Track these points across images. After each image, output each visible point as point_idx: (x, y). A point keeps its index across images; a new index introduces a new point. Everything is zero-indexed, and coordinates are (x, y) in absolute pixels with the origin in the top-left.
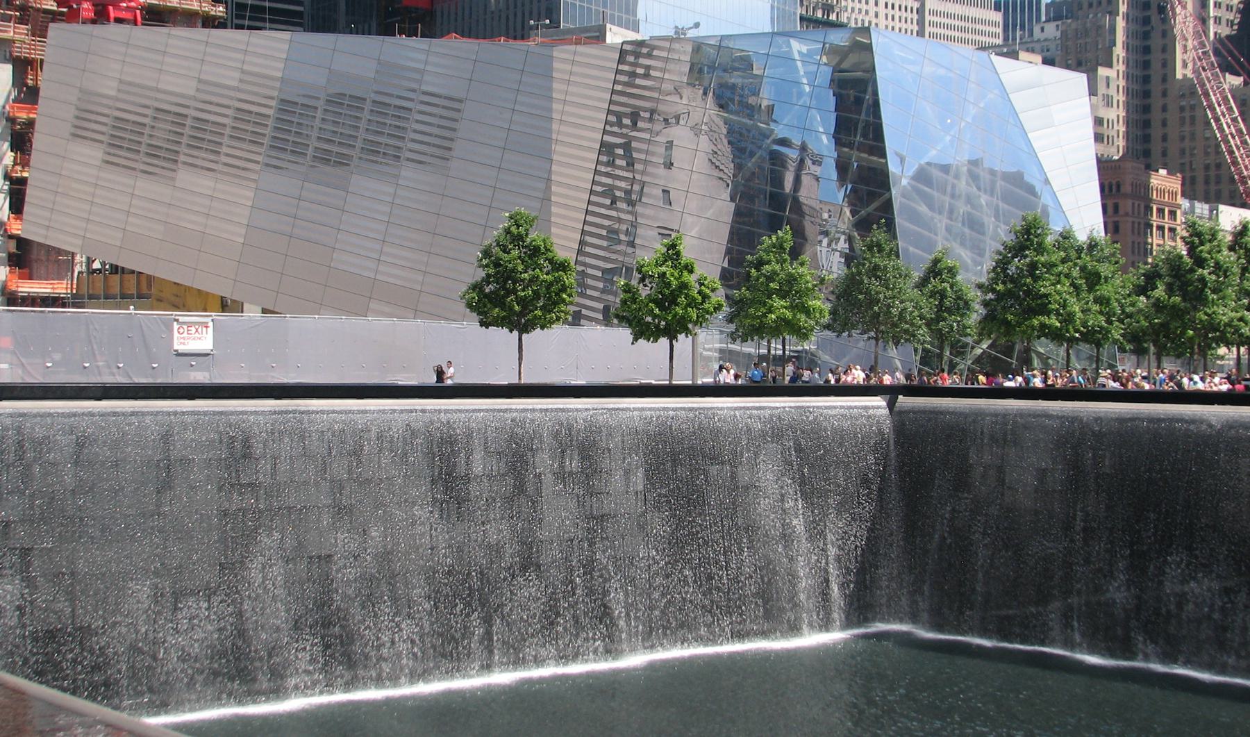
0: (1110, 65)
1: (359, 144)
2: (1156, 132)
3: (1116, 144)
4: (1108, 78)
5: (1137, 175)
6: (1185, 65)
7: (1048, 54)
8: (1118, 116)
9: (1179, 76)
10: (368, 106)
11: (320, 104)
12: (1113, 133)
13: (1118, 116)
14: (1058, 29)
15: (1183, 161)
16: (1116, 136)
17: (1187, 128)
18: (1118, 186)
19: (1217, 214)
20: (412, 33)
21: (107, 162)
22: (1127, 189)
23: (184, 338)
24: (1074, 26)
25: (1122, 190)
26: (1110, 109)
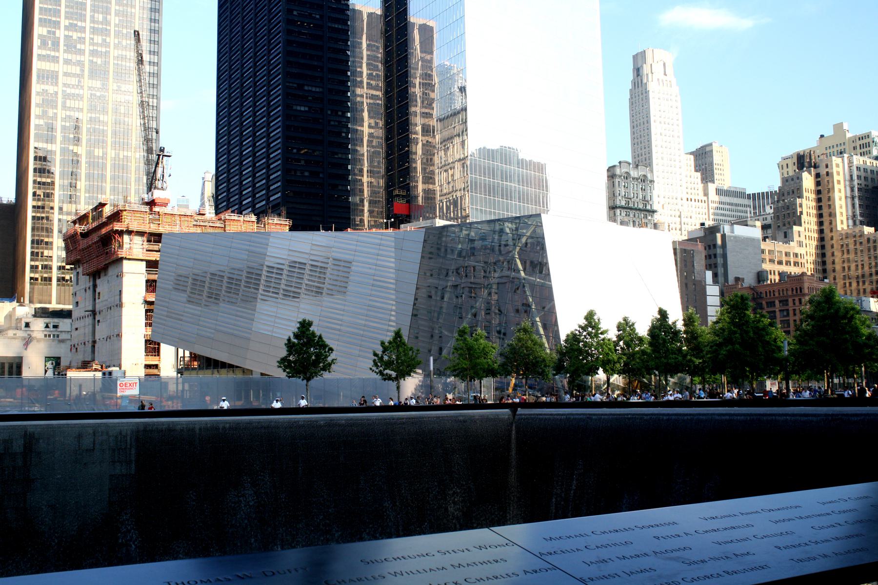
0: (800, 225)
1: (304, 286)
2: (829, 259)
3: (806, 267)
4: (799, 232)
5: (811, 283)
6: (842, 222)
7: (765, 222)
8: (807, 252)
9: (839, 228)
10: (308, 267)
11: (286, 268)
12: (804, 261)
13: (807, 252)
14: (771, 208)
15: (844, 274)
16: (806, 262)
17: (845, 256)
18: (801, 289)
19: (861, 302)
20: (328, 229)
21: (189, 301)
22: (806, 291)
23: (123, 389)
24: (780, 205)
25: (803, 292)
26: (801, 248)
